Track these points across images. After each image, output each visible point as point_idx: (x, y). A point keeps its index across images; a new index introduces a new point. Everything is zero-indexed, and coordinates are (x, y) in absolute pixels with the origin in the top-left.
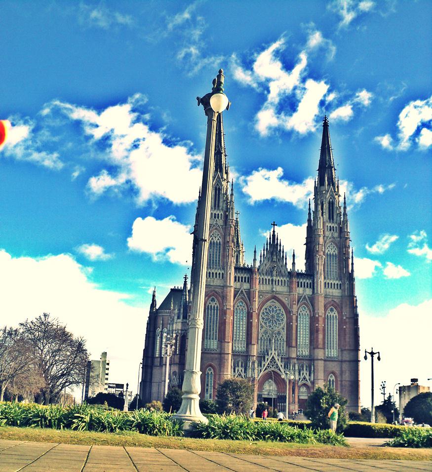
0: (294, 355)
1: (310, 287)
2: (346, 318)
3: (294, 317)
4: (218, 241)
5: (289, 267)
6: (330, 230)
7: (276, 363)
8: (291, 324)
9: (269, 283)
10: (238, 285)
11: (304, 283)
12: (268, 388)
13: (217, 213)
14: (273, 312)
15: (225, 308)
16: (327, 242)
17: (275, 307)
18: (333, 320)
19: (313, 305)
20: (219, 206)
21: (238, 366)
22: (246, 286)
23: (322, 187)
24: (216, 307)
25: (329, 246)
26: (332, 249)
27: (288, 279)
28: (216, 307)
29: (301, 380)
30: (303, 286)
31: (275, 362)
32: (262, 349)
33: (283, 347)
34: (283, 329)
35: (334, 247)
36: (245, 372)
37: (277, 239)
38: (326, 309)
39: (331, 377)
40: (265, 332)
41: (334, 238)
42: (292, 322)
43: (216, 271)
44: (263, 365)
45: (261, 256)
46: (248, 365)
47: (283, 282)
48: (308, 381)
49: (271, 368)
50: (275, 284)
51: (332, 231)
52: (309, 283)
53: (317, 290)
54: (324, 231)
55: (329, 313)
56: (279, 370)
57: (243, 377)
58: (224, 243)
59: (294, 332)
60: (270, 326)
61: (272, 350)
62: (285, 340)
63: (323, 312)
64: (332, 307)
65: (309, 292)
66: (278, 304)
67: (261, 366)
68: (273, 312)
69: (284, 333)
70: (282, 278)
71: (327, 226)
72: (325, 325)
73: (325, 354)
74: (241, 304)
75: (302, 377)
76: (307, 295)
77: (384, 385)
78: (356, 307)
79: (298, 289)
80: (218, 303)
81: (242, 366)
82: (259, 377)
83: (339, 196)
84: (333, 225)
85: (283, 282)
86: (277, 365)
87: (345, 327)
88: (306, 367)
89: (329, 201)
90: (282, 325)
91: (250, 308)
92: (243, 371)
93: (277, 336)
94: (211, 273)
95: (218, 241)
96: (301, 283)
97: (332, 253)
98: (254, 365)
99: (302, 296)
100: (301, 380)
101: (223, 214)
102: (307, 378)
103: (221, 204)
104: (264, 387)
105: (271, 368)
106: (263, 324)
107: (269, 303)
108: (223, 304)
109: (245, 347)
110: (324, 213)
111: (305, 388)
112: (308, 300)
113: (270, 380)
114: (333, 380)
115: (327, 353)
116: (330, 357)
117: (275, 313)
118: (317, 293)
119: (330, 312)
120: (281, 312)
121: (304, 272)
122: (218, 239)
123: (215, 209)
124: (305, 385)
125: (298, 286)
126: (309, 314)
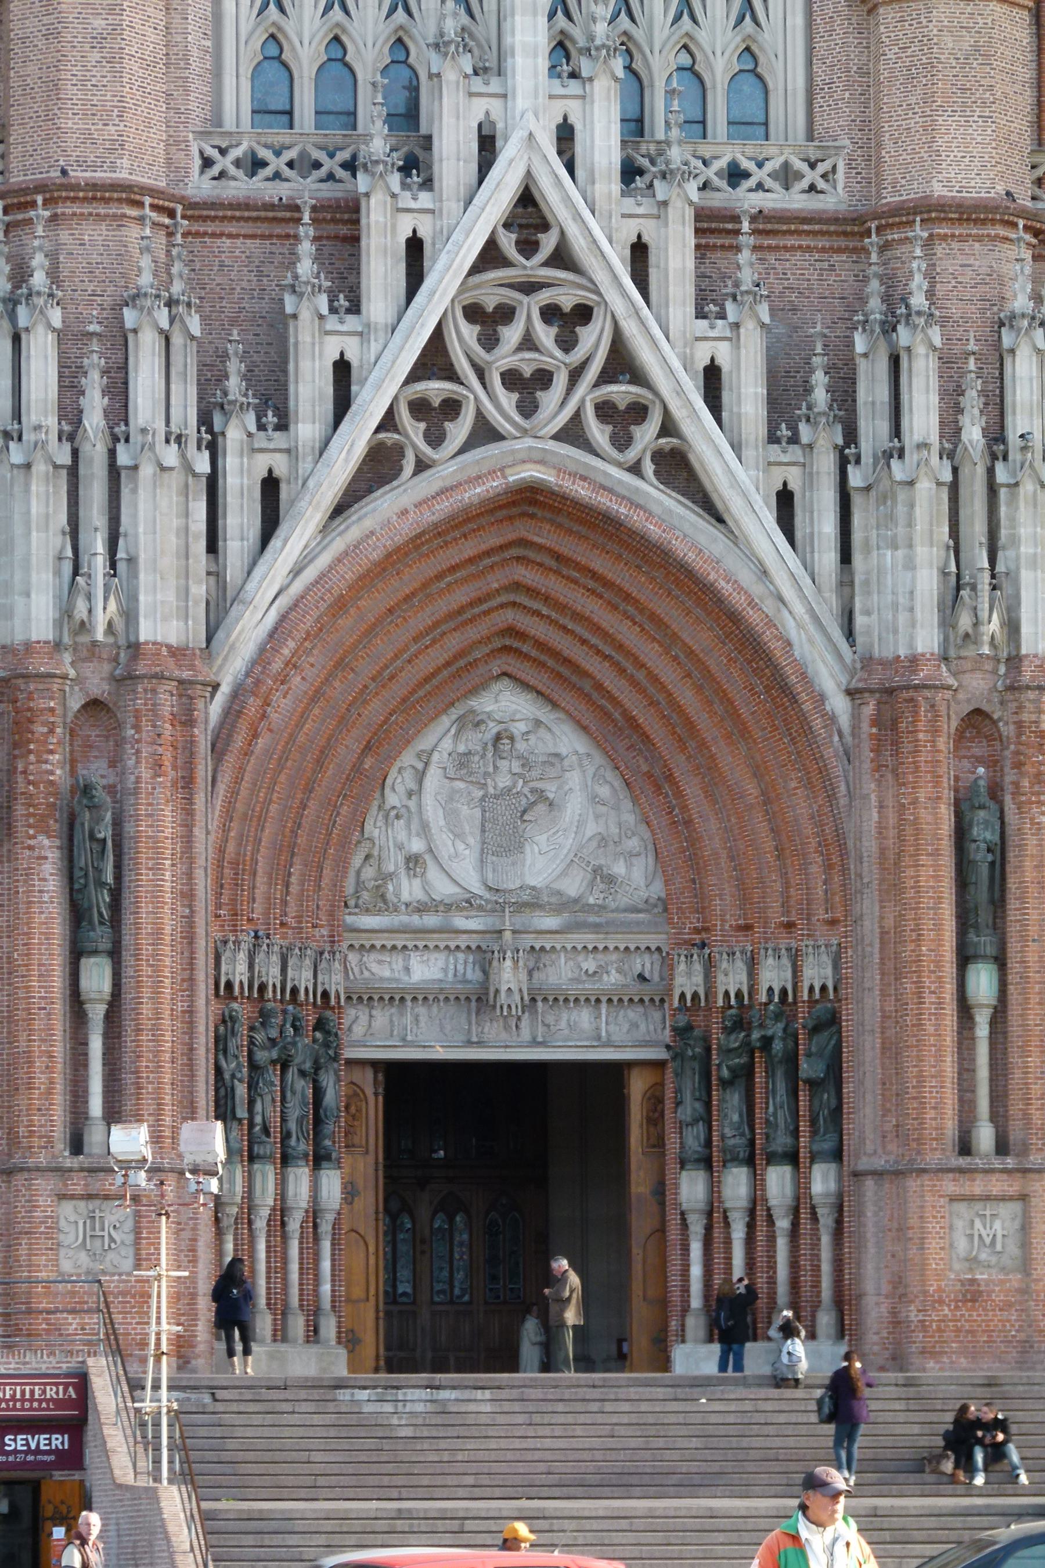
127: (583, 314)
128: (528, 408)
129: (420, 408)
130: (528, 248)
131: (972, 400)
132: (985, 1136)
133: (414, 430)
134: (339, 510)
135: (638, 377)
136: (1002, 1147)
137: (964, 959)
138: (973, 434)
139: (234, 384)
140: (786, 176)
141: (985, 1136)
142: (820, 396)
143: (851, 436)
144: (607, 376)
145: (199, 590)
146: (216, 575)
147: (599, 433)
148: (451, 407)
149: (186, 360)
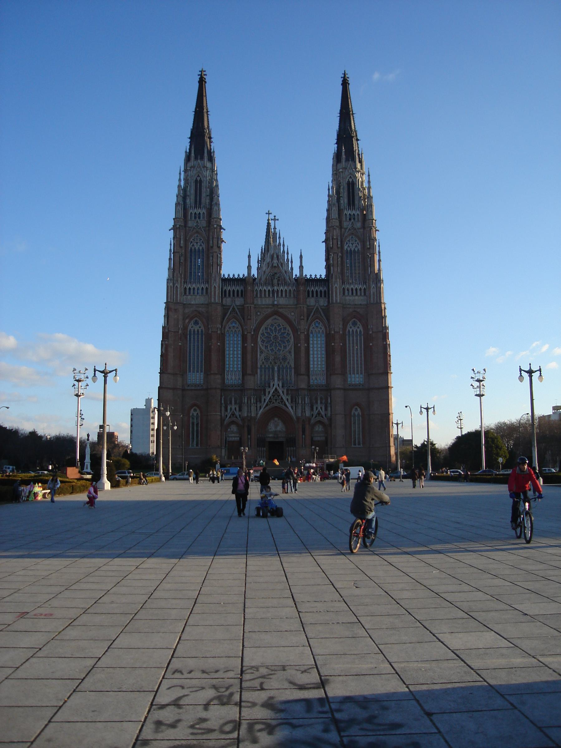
0: (303, 385)
1: (325, 296)
2: (373, 332)
3: (302, 337)
4: (201, 248)
5: (296, 272)
6: (350, 219)
7: (280, 397)
8: (299, 345)
9: (269, 295)
10: (228, 301)
11: (317, 291)
12: (273, 429)
13: (197, 213)
14: (275, 332)
15: (210, 332)
16: (346, 234)
17: (279, 325)
18: (357, 336)
19: (328, 320)
21: (231, 403)
22: (239, 301)
23: (339, 165)
24: (200, 331)
25: (349, 241)
26: (352, 244)
27: (294, 288)
28: (200, 331)
29: (314, 417)
30: (315, 295)
31: (279, 396)
32: (263, 379)
33: (290, 376)
34: (290, 352)
36: (240, 410)
37: (280, 238)
38: (345, 322)
39: (356, 410)
40: (267, 359)
42: (300, 343)
43: (194, 286)
44: (263, 400)
46: (243, 401)
48: (324, 417)
49: (273, 403)
50: (277, 296)
51: (352, 220)
53: (332, 300)
54: (340, 222)
55: (351, 328)
56: (285, 405)
57: (238, 417)
58: (208, 250)
59: (303, 354)
60: (272, 350)
61: (274, 380)
62: (293, 366)
63: (341, 326)
64: (354, 319)
65: (323, 302)
66: (281, 321)
67: (261, 402)
68: (275, 332)
69: (291, 358)
70: (286, 288)
72: (345, 344)
73: (345, 380)
74: (234, 325)
75: (315, 412)
77: (460, 417)
78: (385, 317)
79: (308, 300)
80: (203, 328)
81: (235, 403)
82: (259, 415)
83: (363, 174)
84: (354, 212)
86: (282, 398)
87: (371, 344)
88: (321, 399)
89: (349, 181)
90: (288, 348)
91: (245, 329)
92: (237, 409)
94: (192, 288)
95: (201, 248)
97: (353, 249)
98: (251, 400)
99: (313, 309)
100: (314, 417)
101: (205, 212)
102: (323, 413)
103: (203, 200)
104: (269, 428)
105: (273, 403)
106: (263, 348)
107: (269, 321)
108: (208, 325)
109: (241, 379)
110: (341, 198)
111: (321, 426)
112: (322, 313)
113: (276, 419)
114: (358, 414)
115: (349, 379)
117: (279, 333)
118: (333, 303)
119: (353, 327)
120: (287, 331)
121: (323, 277)
122: (201, 245)
123: (196, 207)
124: (320, 422)
125: (309, 296)
126: (324, 329)
127: (280, 395)
128: (276, 401)
129: (269, 401)
130: (276, 391)
131: (303, 401)
132: (304, 446)
133: (269, 403)
134: (265, 408)
135: (283, 399)
136: (305, 446)
137: (302, 435)
139: (258, 400)
140: (293, 387)
141: (304, 446)
142: (294, 400)
143: (296, 402)
144: (281, 399)
145: (256, 413)
146: (257, 412)
147: (280, 403)
148: (271, 401)
149: (255, 399)
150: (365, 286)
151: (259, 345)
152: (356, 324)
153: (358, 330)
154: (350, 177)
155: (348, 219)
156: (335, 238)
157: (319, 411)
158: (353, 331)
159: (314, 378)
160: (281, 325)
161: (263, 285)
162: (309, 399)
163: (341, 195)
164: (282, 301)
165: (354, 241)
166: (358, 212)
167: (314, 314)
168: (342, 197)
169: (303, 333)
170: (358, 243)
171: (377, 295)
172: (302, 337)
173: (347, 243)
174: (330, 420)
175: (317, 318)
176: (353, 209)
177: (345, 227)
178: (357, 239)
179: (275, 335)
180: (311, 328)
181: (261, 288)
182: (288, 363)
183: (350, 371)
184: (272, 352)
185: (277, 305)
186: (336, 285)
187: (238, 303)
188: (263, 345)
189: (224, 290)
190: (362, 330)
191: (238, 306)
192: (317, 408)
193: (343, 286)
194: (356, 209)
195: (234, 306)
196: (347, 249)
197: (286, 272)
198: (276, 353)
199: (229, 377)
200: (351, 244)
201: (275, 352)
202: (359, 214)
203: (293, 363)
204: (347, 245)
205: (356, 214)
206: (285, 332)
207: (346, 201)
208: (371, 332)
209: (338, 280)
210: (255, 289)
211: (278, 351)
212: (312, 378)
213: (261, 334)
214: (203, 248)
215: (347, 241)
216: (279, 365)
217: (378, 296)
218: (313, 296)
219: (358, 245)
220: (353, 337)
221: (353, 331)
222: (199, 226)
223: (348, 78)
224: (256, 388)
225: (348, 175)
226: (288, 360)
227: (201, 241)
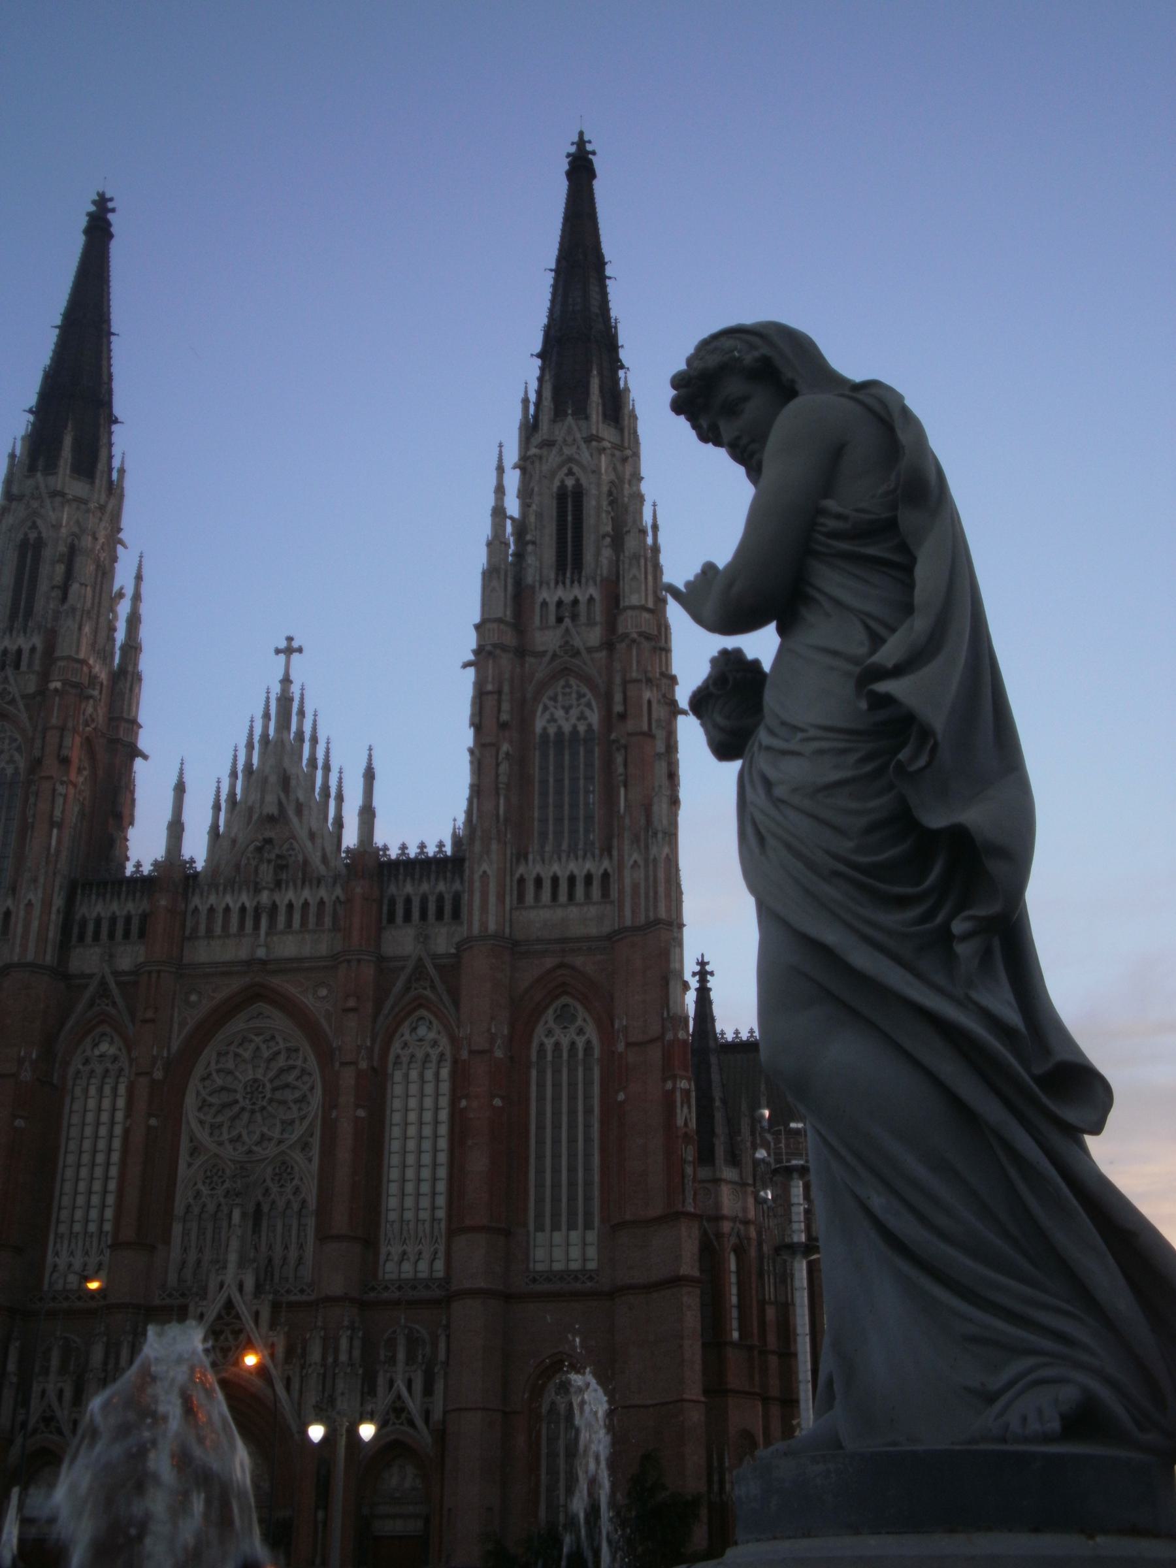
0: (336, 1285)
5: (350, 838)
6: (560, 620)
11: (424, 900)
20: (29, 613)
26: (567, 709)
27: (338, 891)
33: (301, 1247)
34: (305, 1147)
35: (580, 696)
37: (301, 713)
41: (576, 653)
45: (217, 807)
47: (313, 909)
48: (419, 1423)
51: (567, 621)
52: (448, 899)
55: (549, 1033)
62: (312, 1203)
66: (279, 1021)
69: (308, 1167)
70: (306, 893)
71: (544, 604)
76: (435, 956)
84: (576, 592)
85: (313, 909)
87: (621, 1097)
89: (563, 486)
90: (299, 1130)
92: (68, 1395)
93: (275, 1189)
96: (408, 901)
97: (567, 728)
102: (414, 1406)
103: (39, 604)
115: (540, 1253)
116: (550, 1276)
119: (557, 1031)
125: (391, 919)
126: (448, 1048)
127: (241, 1331)
130: (228, 1314)
132: (318, 1560)
138: (330, 1360)
140: (302, 1291)
141: (318, 1560)
142: (299, 1351)
150: (606, 864)
151: (188, 1123)
152: (574, 1018)
153: (580, 1045)
154: (570, 473)
155: (552, 619)
156: (490, 687)
157: (399, 1397)
158: (557, 1045)
159: (396, 1250)
160: (279, 1039)
161: (221, 888)
162: (357, 1343)
163: (528, 537)
164: (288, 947)
165: (574, 696)
166: (593, 591)
167: (407, 989)
168: (534, 543)
169: (351, 1063)
170: (589, 700)
171: (647, 895)
172: (348, 1078)
173: (546, 708)
174: (441, 1435)
175: (420, 1006)
176: (572, 582)
177: (541, 649)
178: (584, 690)
179: (255, 1080)
180: (396, 1047)
181: (212, 899)
182: (297, 1191)
183: (539, 1215)
184: (235, 1149)
185: (264, 962)
186: (485, 867)
187: (125, 962)
188: (201, 1122)
189: (78, 917)
190: (595, 1042)
191: (124, 973)
192: (391, 1383)
193: (521, 870)
194: (583, 580)
195: (103, 977)
196: (545, 729)
197: (312, 836)
198: (250, 1152)
199: (62, 1262)
200: (563, 707)
201: (245, 1148)
202: (596, 595)
203: (314, 1191)
204: (547, 716)
205: (583, 599)
206: (294, 1067)
207: (549, 554)
208: (621, 1047)
209: (494, 846)
210: (191, 907)
211: (258, 1143)
212: (391, 1249)
213: (203, 1079)
214: (16, 769)
215: (545, 700)
216: (258, 1205)
217: (651, 894)
218: (407, 917)
219: (588, 713)
220: (557, 1071)
221: (557, 1045)
222: (10, 693)
223: (594, 153)
224: (157, 1302)
225: (560, 467)
226: (296, 1182)
227: (15, 745)
